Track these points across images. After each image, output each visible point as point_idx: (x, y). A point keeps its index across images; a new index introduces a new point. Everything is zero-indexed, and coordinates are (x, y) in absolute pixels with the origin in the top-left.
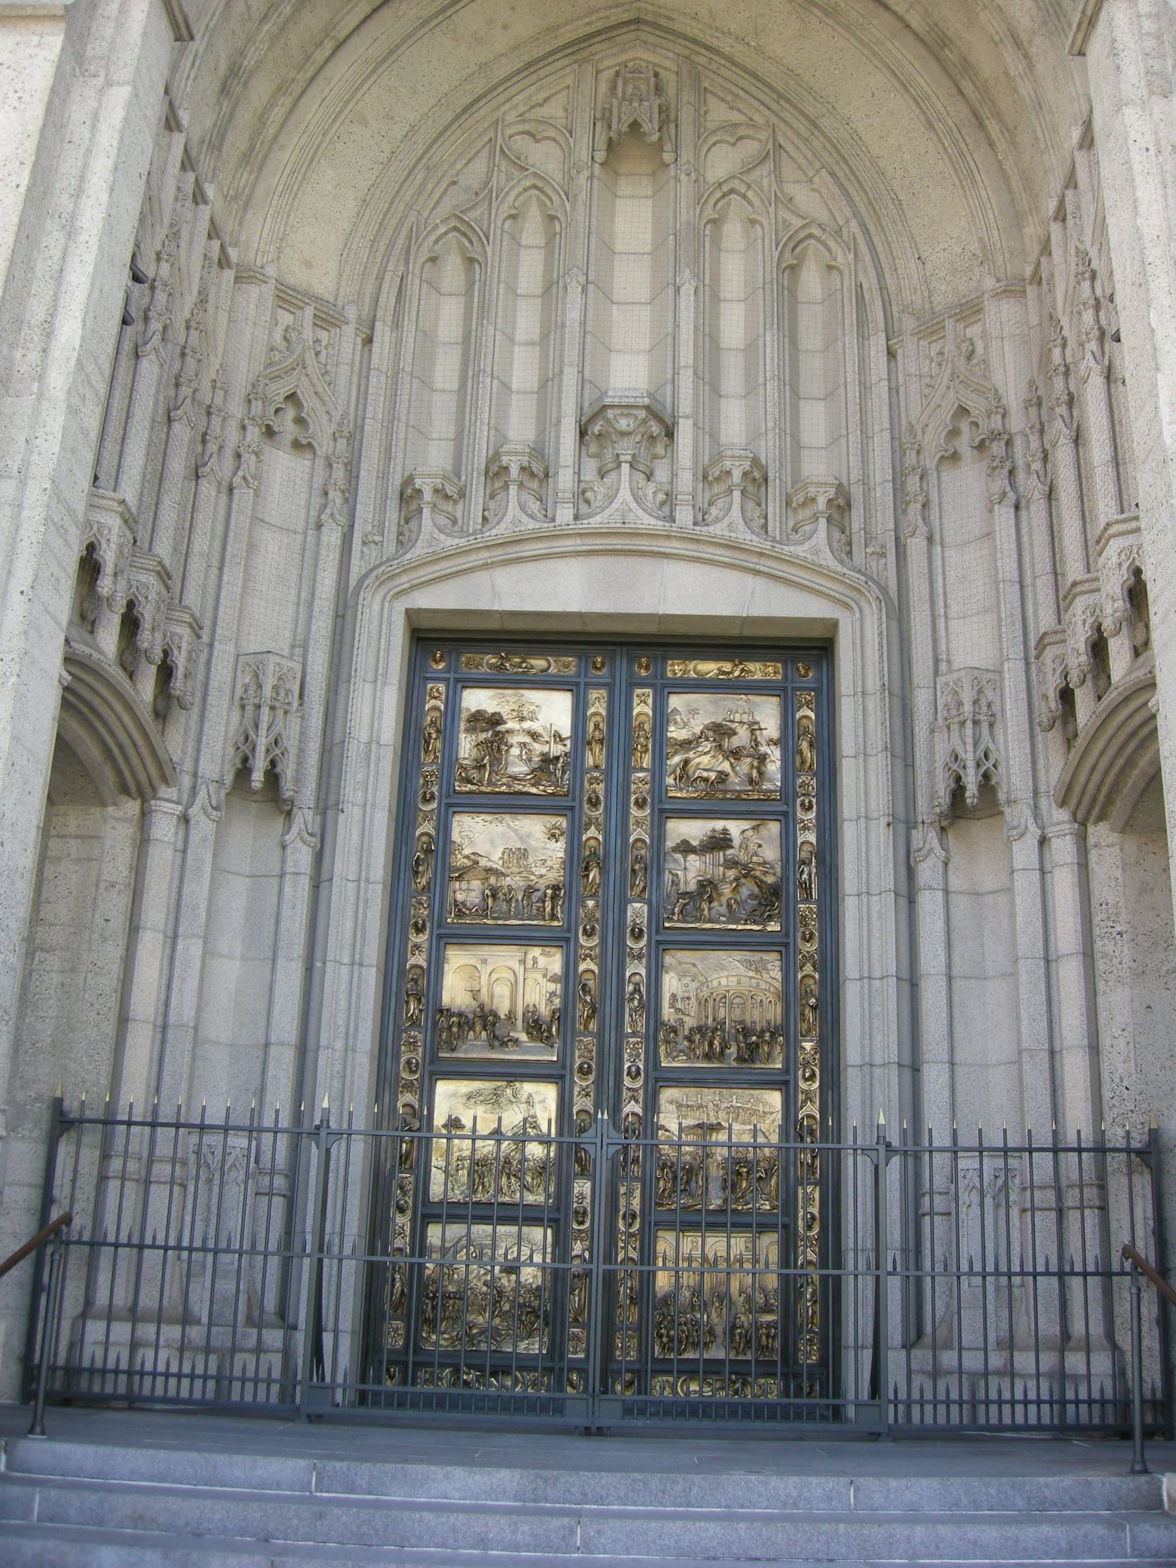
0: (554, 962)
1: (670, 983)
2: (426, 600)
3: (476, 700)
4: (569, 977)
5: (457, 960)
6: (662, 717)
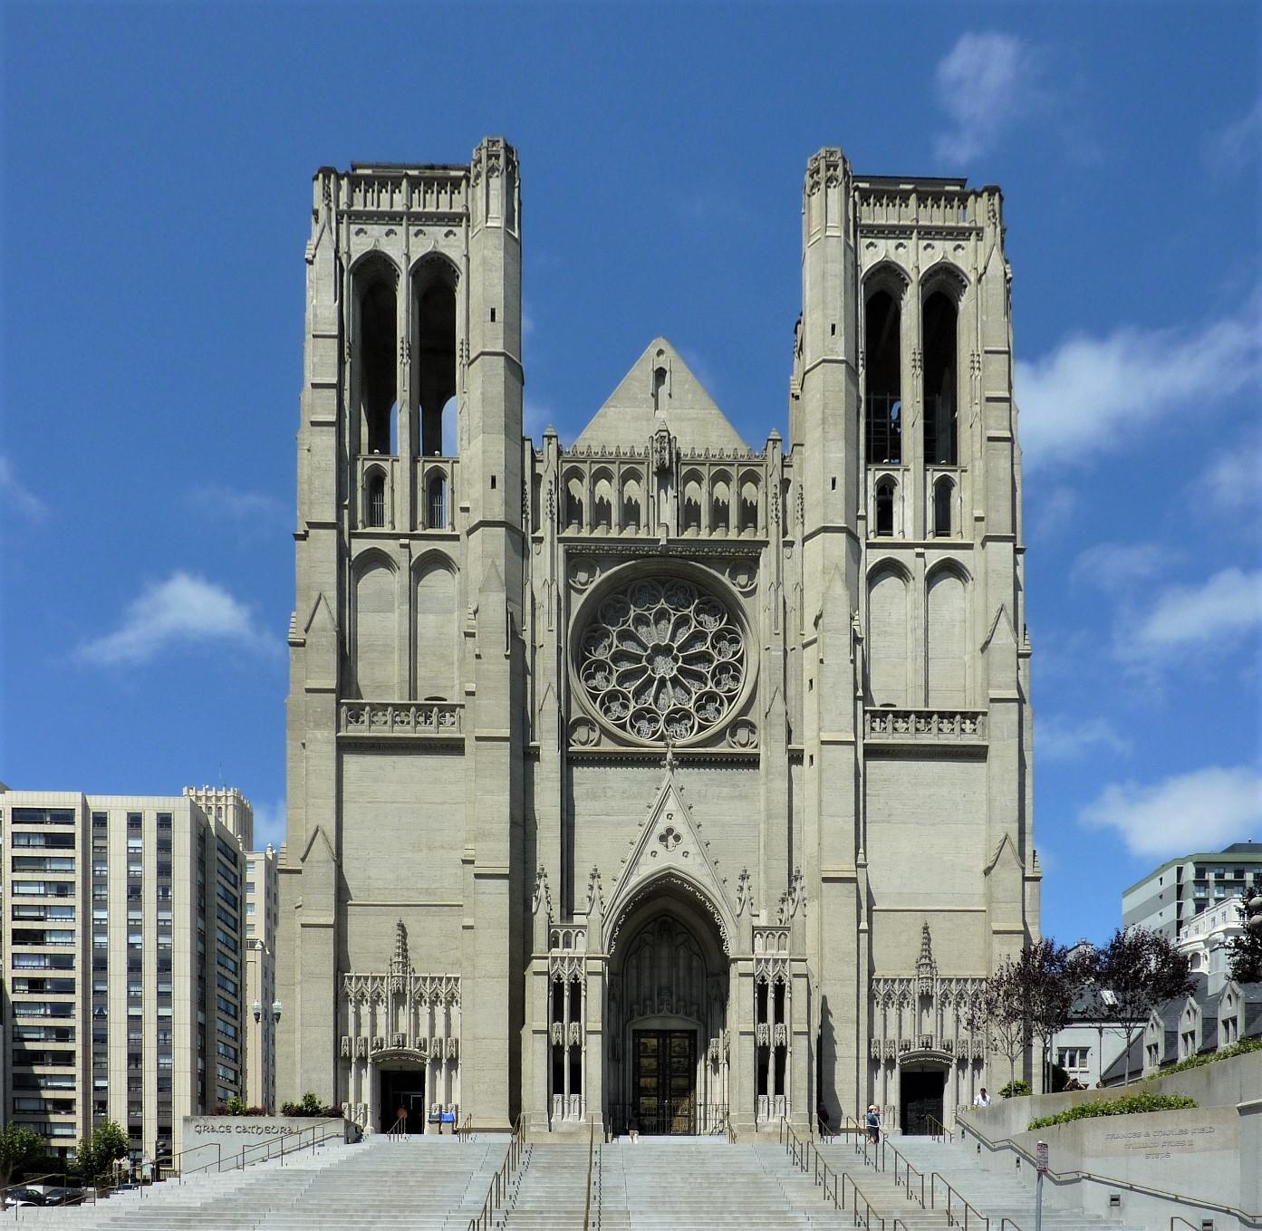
0: (655, 1080)
1: (673, 1083)
2: (638, 1027)
3: (642, 1040)
4: (658, 1082)
5: (642, 1080)
6: (671, 1043)
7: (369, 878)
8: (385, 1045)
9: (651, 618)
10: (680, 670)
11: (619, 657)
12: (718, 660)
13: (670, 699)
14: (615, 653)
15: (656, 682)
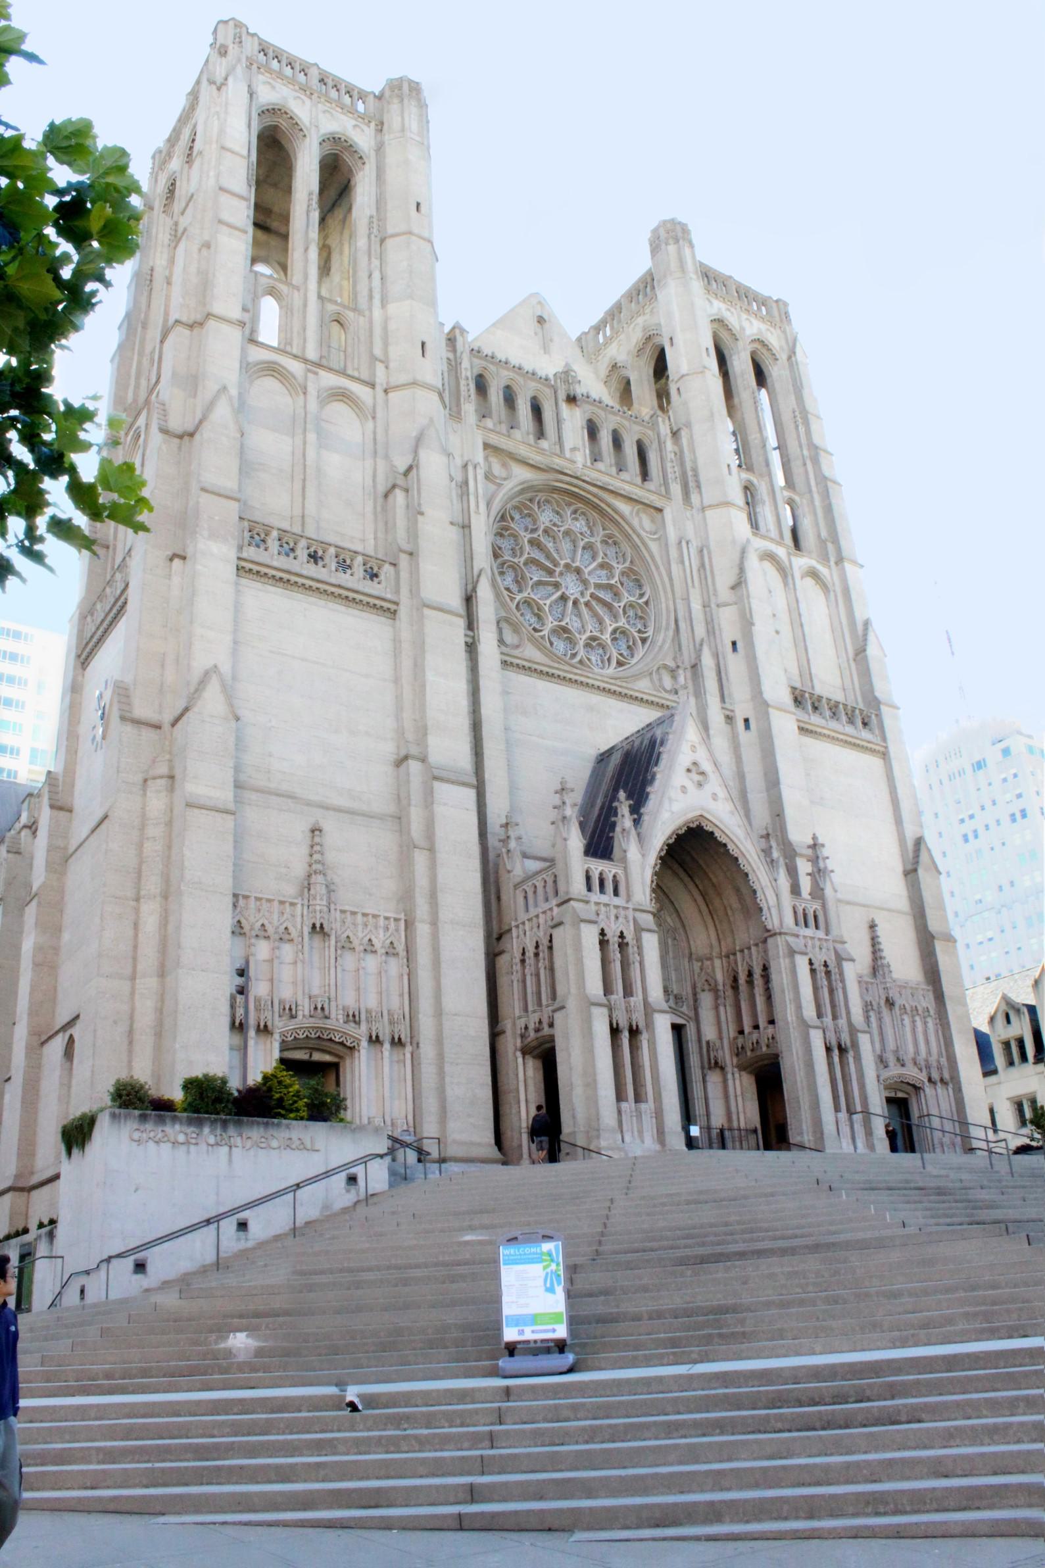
7: (270, 755)
8: (300, 1013)
9: (560, 535)
10: (592, 595)
11: (532, 561)
12: (626, 598)
13: (583, 626)
14: (527, 559)
15: (570, 603)
